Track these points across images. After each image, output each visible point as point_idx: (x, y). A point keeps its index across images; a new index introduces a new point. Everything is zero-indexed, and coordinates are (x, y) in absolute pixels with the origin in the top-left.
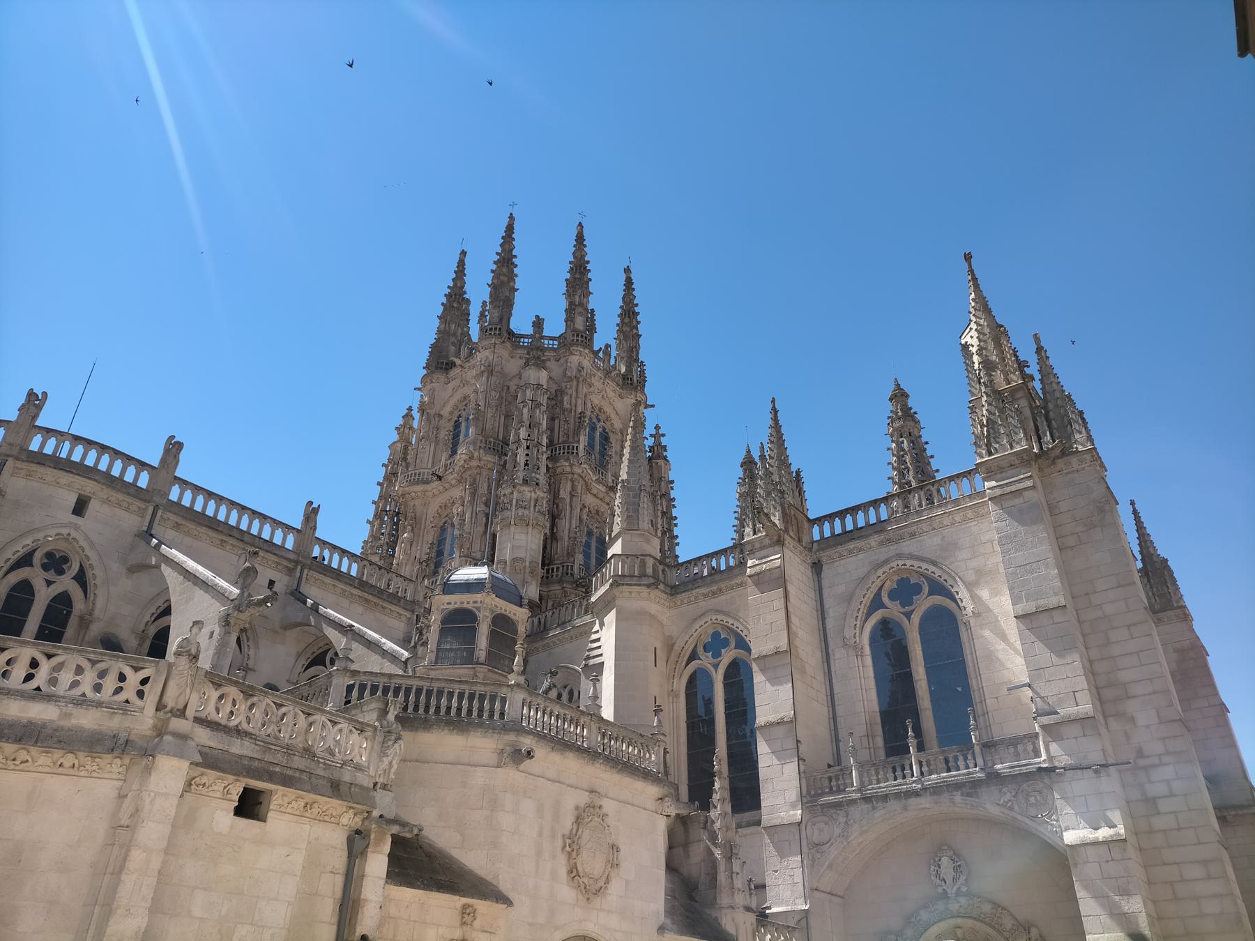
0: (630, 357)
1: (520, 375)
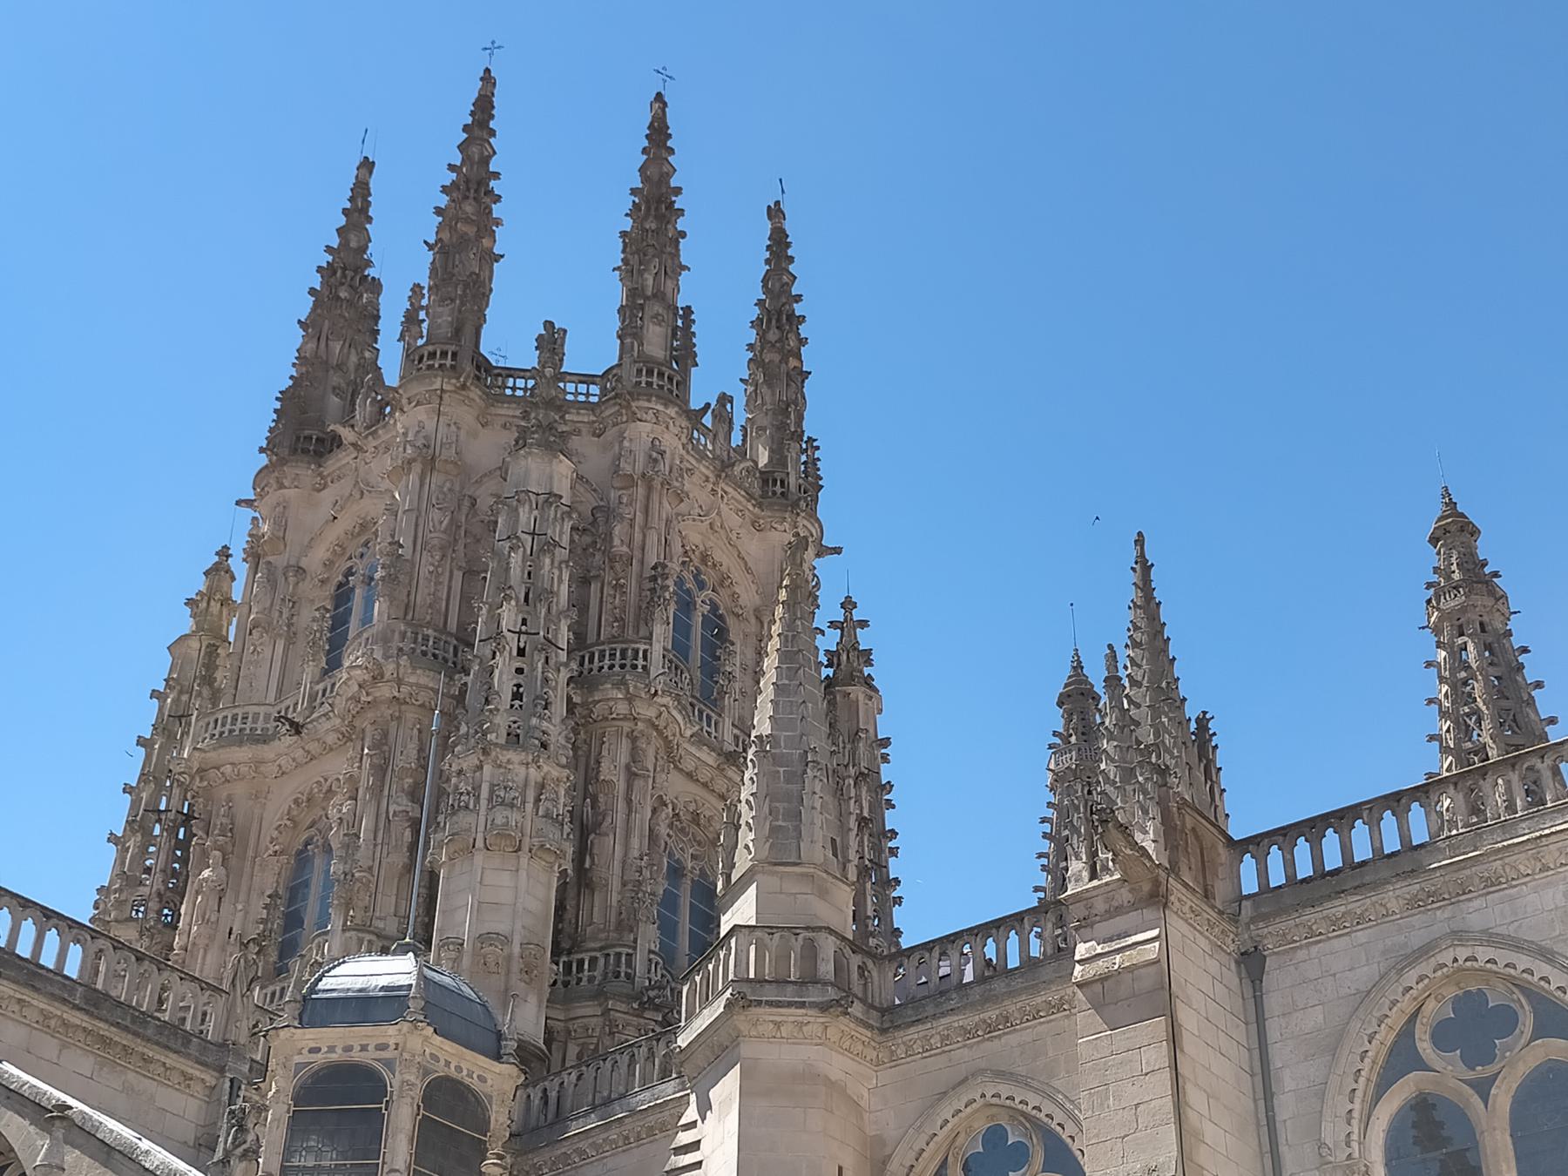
0: (781, 427)
1: (503, 471)
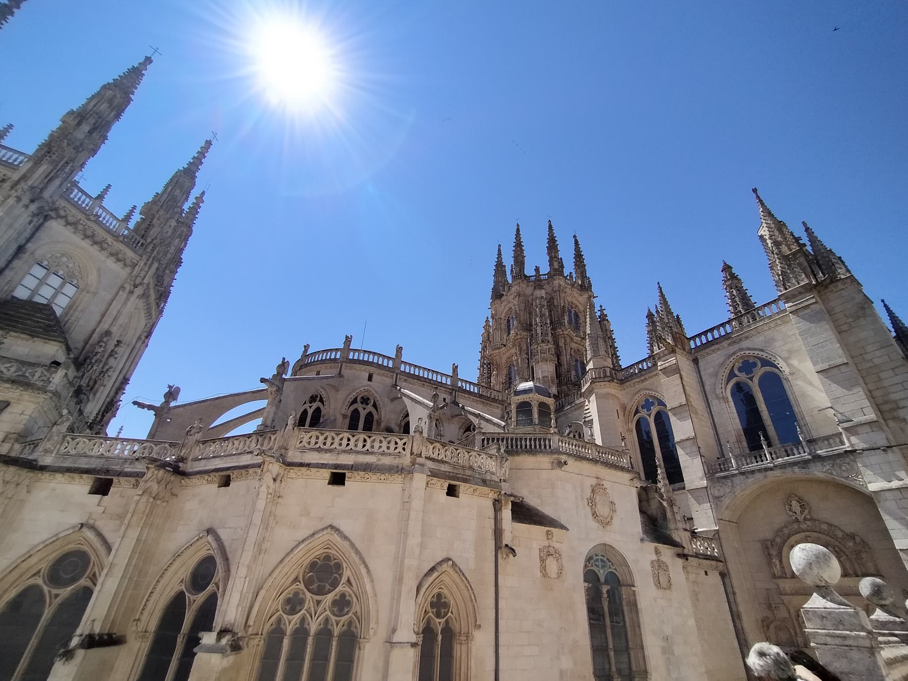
0: (582, 276)
1: (532, 294)
